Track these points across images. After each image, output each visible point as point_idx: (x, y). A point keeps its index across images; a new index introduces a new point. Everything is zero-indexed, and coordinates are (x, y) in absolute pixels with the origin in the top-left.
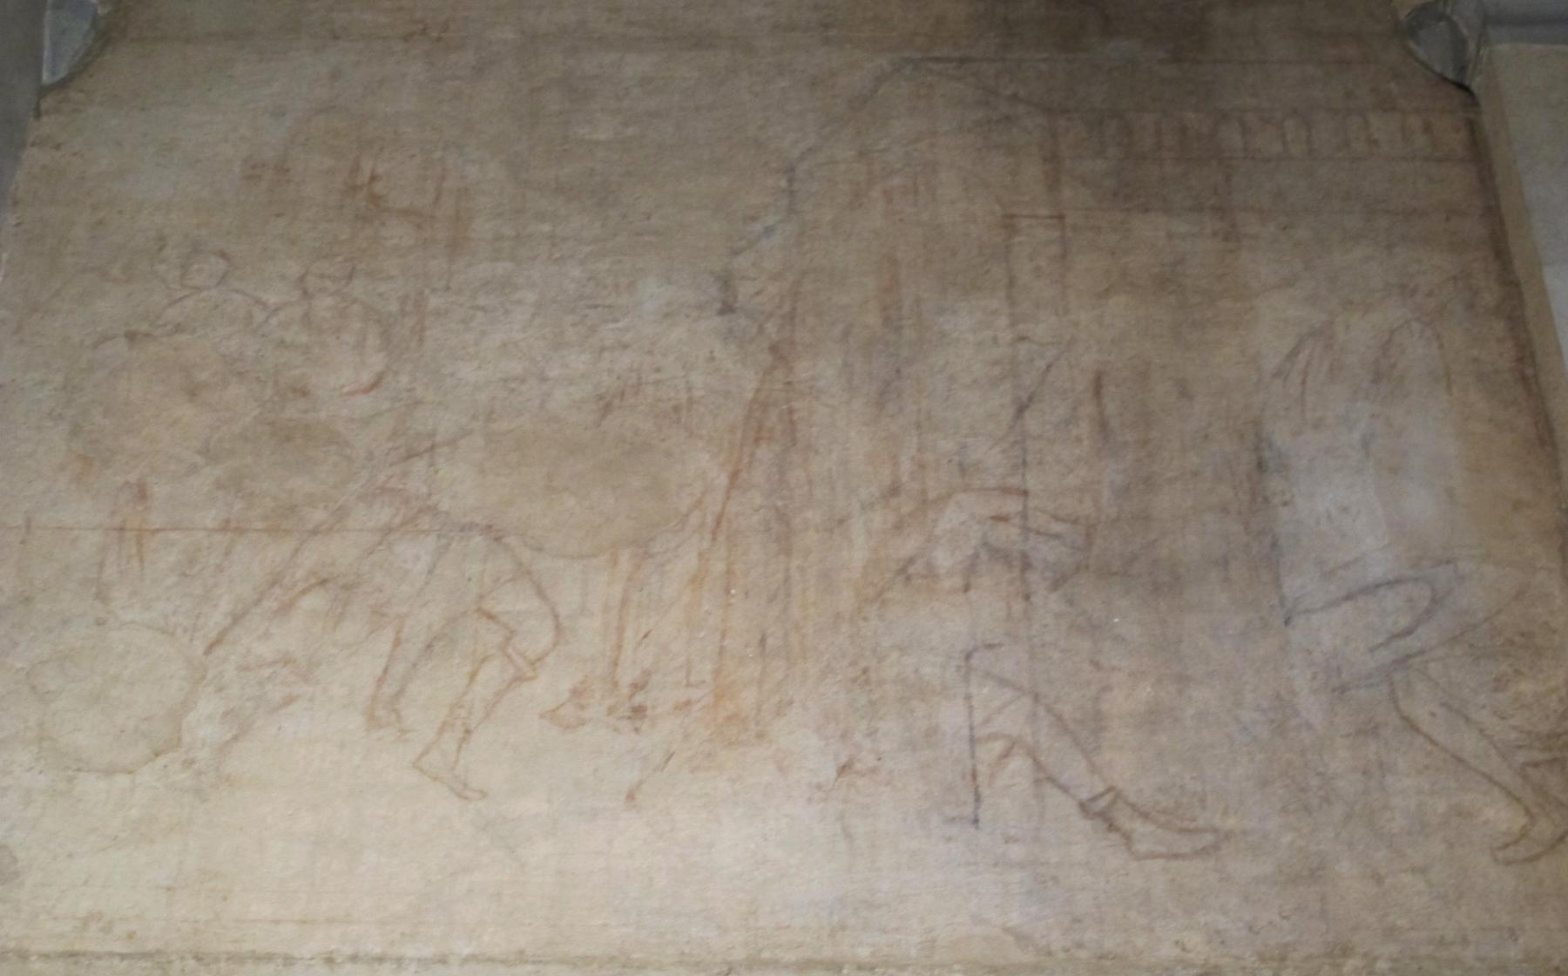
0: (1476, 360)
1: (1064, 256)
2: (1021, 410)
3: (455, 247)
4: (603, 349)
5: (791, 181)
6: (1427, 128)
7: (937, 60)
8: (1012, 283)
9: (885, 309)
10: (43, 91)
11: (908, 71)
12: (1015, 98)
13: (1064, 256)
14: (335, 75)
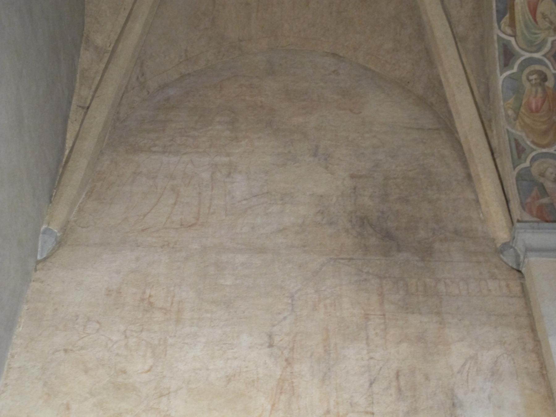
0: (526, 368)
1: (385, 329)
2: (371, 384)
3: (178, 321)
4: (228, 359)
5: (292, 301)
6: (508, 286)
7: (342, 259)
8: (368, 338)
9: (325, 346)
10: (38, 262)
11: (332, 263)
12: (368, 273)
13: (385, 329)
14: (137, 259)
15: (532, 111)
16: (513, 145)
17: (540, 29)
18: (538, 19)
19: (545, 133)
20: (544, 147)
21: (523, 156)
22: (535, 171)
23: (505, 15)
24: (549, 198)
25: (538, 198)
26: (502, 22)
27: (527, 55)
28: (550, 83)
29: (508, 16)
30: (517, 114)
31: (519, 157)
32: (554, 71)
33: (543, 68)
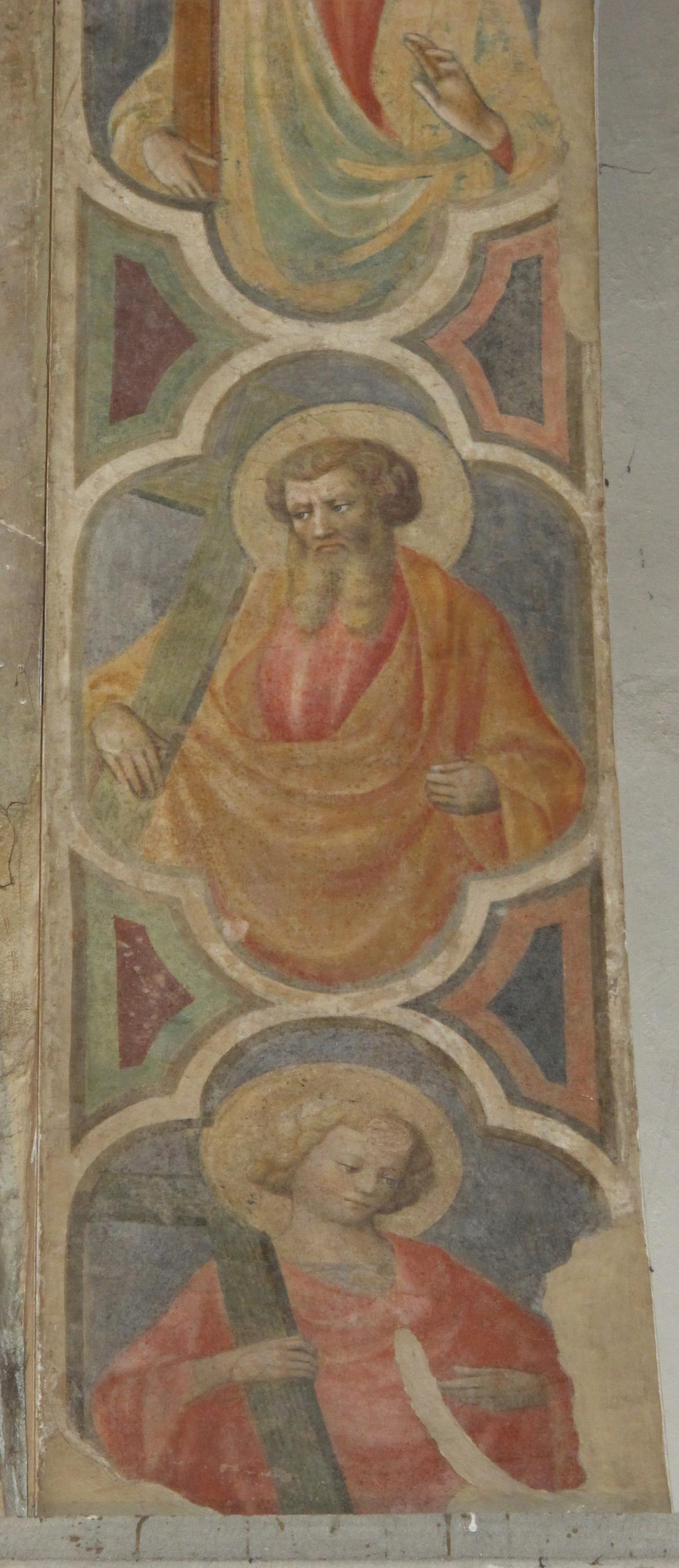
15: (279, 729)
16: (104, 964)
17: (399, 155)
18: (381, 89)
19: (360, 879)
20: (326, 979)
21: (162, 1047)
22: (228, 1153)
23: (153, 59)
24: (295, 1341)
25: (211, 1343)
26: (120, 106)
27: (289, 335)
28: (438, 534)
29: (165, 63)
30: (165, 749)
31: (132, 1054)
32: (482, 451)
33: (397, 431)
